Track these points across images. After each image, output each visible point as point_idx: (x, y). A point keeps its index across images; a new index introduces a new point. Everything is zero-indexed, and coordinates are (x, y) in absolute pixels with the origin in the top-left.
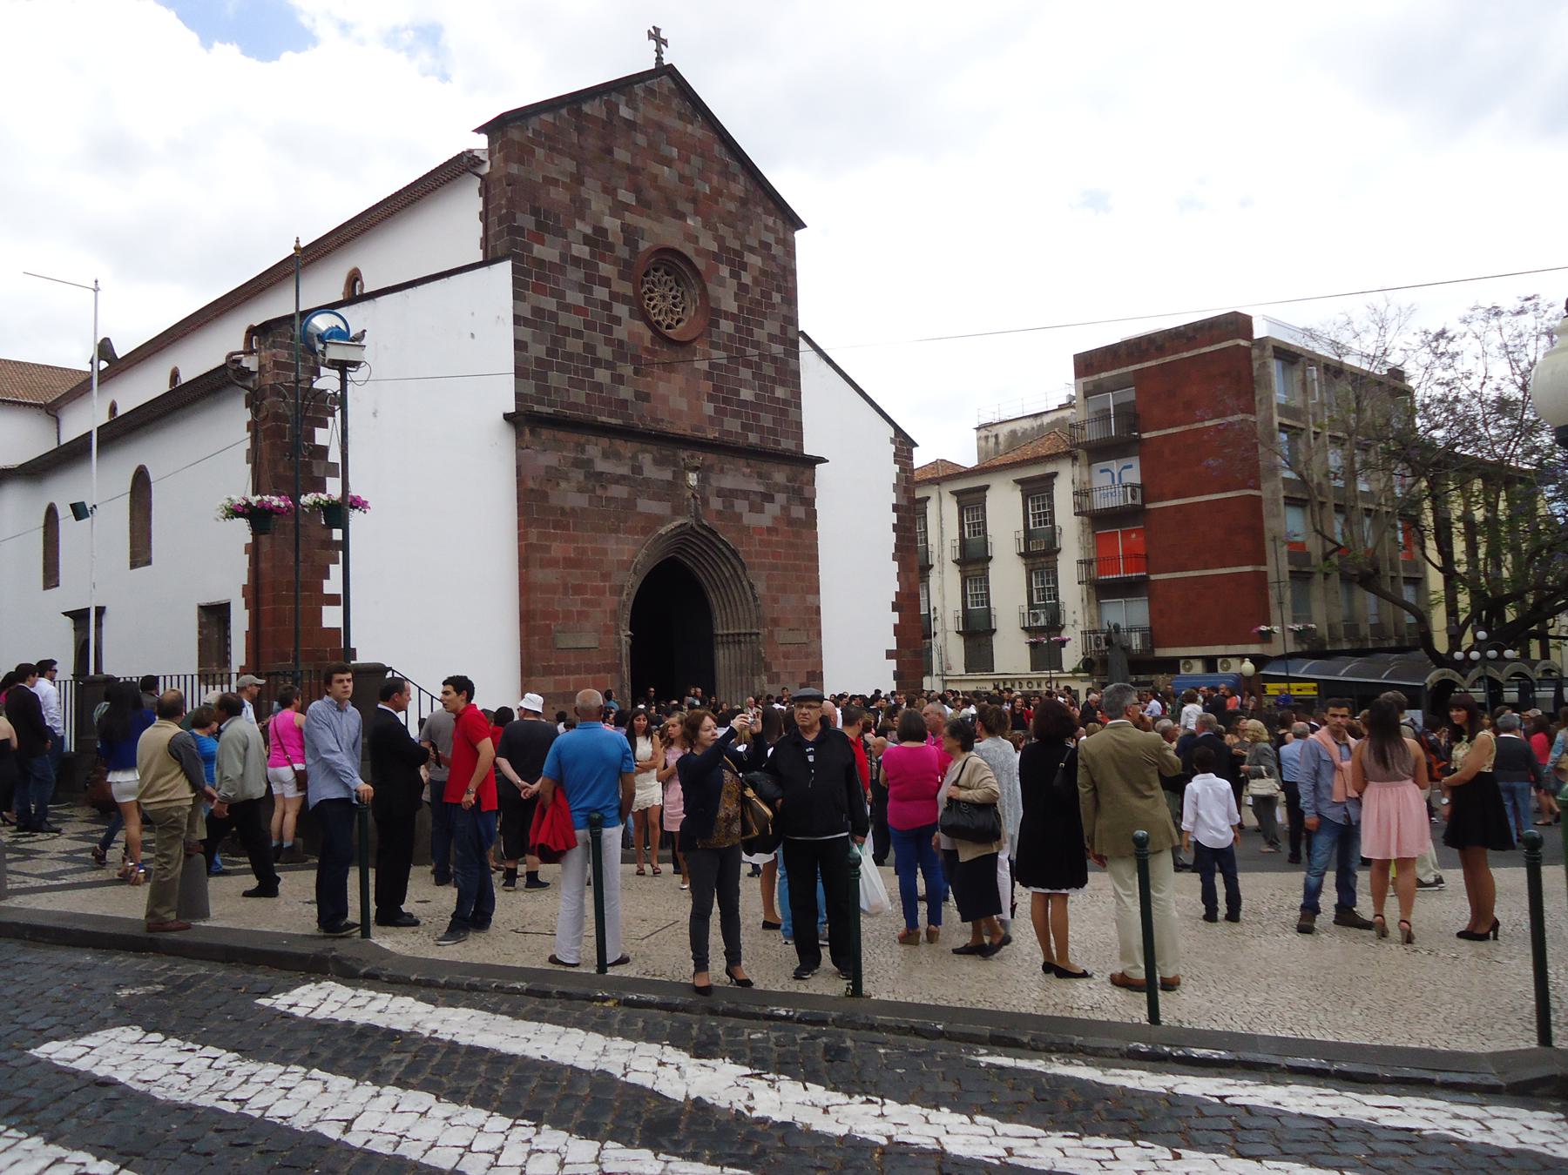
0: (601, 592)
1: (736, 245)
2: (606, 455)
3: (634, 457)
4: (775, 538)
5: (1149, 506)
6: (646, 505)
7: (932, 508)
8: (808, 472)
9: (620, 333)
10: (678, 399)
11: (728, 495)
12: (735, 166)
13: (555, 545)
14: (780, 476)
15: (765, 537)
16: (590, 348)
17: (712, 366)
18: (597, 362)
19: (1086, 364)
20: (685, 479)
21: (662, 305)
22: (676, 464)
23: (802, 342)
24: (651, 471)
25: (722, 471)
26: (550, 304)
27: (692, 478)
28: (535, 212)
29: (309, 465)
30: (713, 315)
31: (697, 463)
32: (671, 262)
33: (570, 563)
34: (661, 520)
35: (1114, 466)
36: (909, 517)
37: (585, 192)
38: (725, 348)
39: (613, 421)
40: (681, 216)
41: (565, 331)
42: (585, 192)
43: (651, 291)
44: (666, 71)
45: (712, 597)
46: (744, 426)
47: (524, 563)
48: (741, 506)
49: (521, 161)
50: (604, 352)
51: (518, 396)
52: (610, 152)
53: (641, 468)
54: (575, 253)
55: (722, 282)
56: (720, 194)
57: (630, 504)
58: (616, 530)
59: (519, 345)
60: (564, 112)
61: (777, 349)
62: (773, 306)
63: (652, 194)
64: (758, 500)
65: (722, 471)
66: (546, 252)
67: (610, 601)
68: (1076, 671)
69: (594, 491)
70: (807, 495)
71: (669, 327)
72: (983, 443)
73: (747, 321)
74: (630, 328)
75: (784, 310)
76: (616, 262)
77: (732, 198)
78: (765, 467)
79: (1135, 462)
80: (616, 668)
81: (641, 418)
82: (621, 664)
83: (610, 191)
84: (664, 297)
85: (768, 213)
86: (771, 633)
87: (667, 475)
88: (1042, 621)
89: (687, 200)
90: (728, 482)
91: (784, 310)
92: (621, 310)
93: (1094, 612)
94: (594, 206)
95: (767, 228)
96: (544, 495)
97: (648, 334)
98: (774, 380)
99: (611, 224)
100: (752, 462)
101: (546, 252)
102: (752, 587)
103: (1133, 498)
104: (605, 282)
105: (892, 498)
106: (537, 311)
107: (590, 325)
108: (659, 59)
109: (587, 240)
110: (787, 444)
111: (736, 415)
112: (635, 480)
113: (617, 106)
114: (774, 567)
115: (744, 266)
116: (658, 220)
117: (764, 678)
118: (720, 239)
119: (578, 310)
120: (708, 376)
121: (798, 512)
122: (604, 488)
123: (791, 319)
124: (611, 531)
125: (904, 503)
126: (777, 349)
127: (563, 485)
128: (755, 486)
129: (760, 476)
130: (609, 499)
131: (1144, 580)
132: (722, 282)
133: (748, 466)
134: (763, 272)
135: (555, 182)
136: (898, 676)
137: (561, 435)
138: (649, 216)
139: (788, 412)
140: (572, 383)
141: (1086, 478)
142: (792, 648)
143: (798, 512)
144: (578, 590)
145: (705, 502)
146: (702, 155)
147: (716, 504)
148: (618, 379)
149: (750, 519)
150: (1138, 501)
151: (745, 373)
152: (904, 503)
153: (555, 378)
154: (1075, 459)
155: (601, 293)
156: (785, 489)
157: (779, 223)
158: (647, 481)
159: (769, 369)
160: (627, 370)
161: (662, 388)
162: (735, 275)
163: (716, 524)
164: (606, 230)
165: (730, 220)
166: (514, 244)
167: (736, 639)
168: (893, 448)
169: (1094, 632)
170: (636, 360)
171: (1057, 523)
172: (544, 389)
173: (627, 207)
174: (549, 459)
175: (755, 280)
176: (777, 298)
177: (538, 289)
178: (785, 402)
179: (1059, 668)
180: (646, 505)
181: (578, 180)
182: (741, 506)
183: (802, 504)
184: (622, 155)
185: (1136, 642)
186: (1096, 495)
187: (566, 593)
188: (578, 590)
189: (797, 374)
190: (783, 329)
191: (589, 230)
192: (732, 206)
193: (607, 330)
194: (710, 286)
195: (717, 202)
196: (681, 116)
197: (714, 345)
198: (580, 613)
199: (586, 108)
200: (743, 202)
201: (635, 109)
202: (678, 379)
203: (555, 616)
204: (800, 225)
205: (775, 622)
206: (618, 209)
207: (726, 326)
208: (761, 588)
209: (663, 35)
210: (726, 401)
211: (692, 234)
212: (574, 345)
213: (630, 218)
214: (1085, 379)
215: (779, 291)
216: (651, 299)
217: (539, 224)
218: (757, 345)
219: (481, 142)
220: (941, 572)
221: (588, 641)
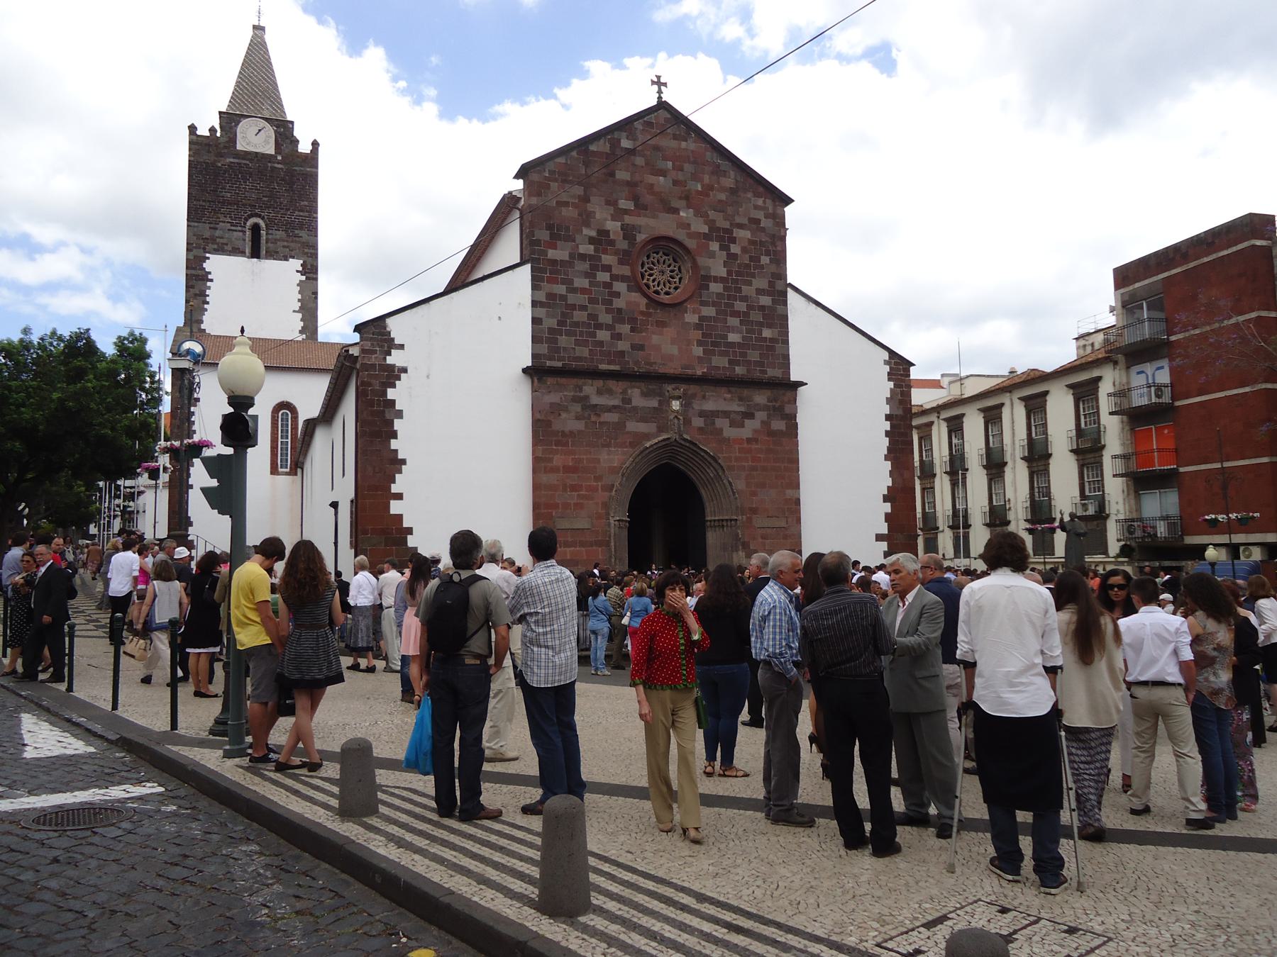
0: (595, 489)
1: (727, 225)
2: (599, 392)
3: (624, 392)
4: (754, 446)
5: (1178, 403)
6: (633, 426)
7: (1006, 413)
8: (789, 394)
9: (619, 303)
10: (669, 346)
11: (709, 416)
12: (725, 165)
13: (556, 457)
14: (760, 398)
15: (745, 445)
16: (593, 317)
17: (701, 318)
18: (599, 326)
19: (1124, 276)
20: (669, 405)
21: (662, 278)
22: (661, 394)
23: (790, 292)
24: (638, 399)
25: (704, 397)
26: (561, 289)
27: (676, 405)
28: (550, 227)
29: (383, 412)
30: (704, 280)
31: (677, 393)
32: (665, 246)
33: (567, 469)
34: (647, 437)
35: (1149, 368)
36: (904, 424)
37: (590, 207)
39: (612, 367)
40: (676, 211)
41: (573, 307)
42: (590, 207)
43: (651, 269)
44: (662, 105)
45: (703, 492)
46: (730, 362)
47: (535, 471)
48: (721, 423)
49: (539, 194)
50: (605, 318)
51: (534, 356)
52: (612, 175)
53: (629, 401)
54: (581, 251)
55: (712, 255)
56: (711, 188)
57: (620, 426)
58: (608, 445)
59: (536, 321)
60: (574, 153)
61: (766, 301)
62: (762, 267)
63: (648, 199)
64: (739, 418)
65: (704, 397)
66: (559, 254)
67: (602, 496)
68: (1118, 556)
69: (589, 418)
70: (788, 410)
71: (667, 293)
72: (1082, 352)
74: (627, 298)
75: (773, 268)
76: (616, 253)
77: (723, 189)
78: (746, 392)
79: (1165, 363)
80: (608, 544)
81: (637, 363)
82: (609, 542)
83: (611, 203)
84: (663, 272)
85: (757, 195)
86: (750, 520)
87: (654, 403)
88: (1091, 511)
89: (680, 198)
90: (710, 406)
91: (773, 268)
92: (620, 287)
93: (1133, 502)
94: (598, 216)
95: (756, 207)
96: (549, 423)
97: (644, 301)
98: (761, 324)
99: (613, 226)
100: (733, 389)
101: (559, 254)
102: (730, 483)
103: (1158, 396)
104: (607, 268)
106: (551, 296)
107: (593, 301)
108: (660, 98)
109: (592, 241)
110: (773, 373)
112: (626, 409)
113: (619, 141)
114: (754, 469)
115: (733, 240)
117: (742, 554)
119: (583, 291)
120: (698, 327)
121: (778, 425)
122: (599, 416)
123: (782, 275)
124: (604, 446)
125: (900, 412)
126: (766, 301)
127: (564, 415)
128: (736, 407)
129: (741, 399)
131: (1174, 473)
132: (712, 255)
133: (730, 392)
134: (751, 242)
135: (566, 204)
137: (563, 381)
138: (645, 216)
139: (778, 349)
140: (577, 343)
141: (1125, 380)
142: (769, 531)
143: (778, 425)
144: (574, 488)
145: (687, 422)
146: (695, 162)
147: (698, 422)
148: (618, 337)
149: (729, 432)
150: (1166, 398)
151: (734, 321)
152: (900, 412)
153: (564, 341)
154: (1116, 363)
155: (603, 277)
156: (766, 408)
157: (769, 202)
158: (635, 409)
159: (756, 316)
160: (625, 329)
161: (655, 339)
162: (722, 248)
163: (697, 438)
164: (606, 233)
165: (720, 207)
166: (533, 252)
167: (721, 524)
168: (887, 368)
169: (1133, 520)
170: (632, 321)
171: (1102, 422)
172: (555, 350)
173: (626, 212)
174: (554, 398)
175: (744, 250)
176: (765, 260)
177: (550, 281)
179: (1105, 553)
180: (633, 426)
181: (585, 199)
182: (721, 423)
183: (783, 419)
184: (622, 175)
185: (1162, 530)
186: (1134, 394)
187: (565, 490)
188: (574, 488)
189: (785, 318)
190: (771, 284)
191: (593, 234)
192: (723, 196)
193: (611, 302)
194: (702, 261)
195: (708, 195)
196: (675, 137)
198: (576, 504)
199: (593, 148)
200: (733, 191)
201: (634, 140)
202: (670, 332)
203: (556, 506)
204: (788, 201)
205: (754, 511)
206: (619, 214)
207: (715, 288)
208: (740, 485)
209: (662, 80)
210: (714, 344)
211: (686, 223)
212: (580, 316)
214: (1122, 291)
215: (768, 253)
216: (651, 275)
217: (552, 235)
218: (744, 299)
219: (519, 184)
220: (1014, 468)
221: (583, 523)
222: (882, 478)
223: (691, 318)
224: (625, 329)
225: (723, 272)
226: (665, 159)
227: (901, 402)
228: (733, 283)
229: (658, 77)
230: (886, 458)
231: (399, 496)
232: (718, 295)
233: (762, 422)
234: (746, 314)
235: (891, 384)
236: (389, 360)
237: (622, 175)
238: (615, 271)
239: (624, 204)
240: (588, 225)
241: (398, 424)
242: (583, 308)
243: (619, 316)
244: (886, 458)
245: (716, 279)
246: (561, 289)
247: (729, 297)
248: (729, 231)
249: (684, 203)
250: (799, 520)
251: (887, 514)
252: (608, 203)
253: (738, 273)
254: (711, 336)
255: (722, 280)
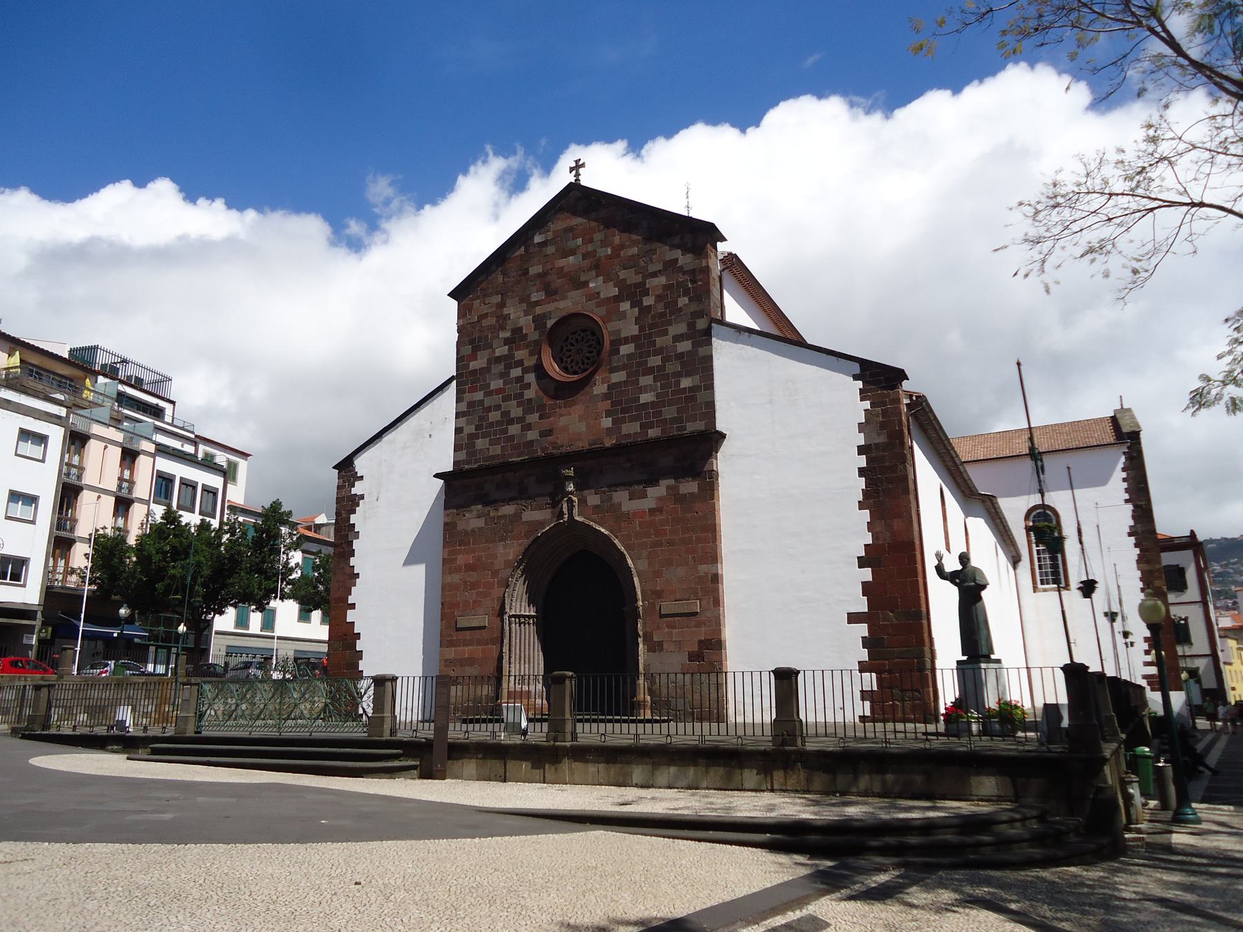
1: (639, 278)
9: (530, 394)
15: (648, 518)
16: (506, 414)
18: (511, 422)
20: (563, 487)
26: (479, 395)
33: (470, 568)
38: (624, 368)
40: (586, 284)
41: (489, 409)
50: (516, 412)
52: (526, 272)
55: (623, 316)
56: (622, 247)
57: (517, 516)
59: (458, 431)
61: (684, 346)
63: (559, 282)
73: (650, 335)
81: (543, 449)
83: (524, 299)
89: (590, 269)
91: (694, 307)
99: (526, 322)
104: (520, 363)
105: (861, 440)
106: (471, 404)
107: (505, 399)
109: (507, 342)
111: (633, 419)
116: (564, 298)
118: (621, 284)
119: (498, 391)
120: (606, 397)
124: (500, 540)
130: (500, 517)
132: (623, 316)
134: (666, 287)
136: (866, 643)
143: (690, 487)
144: (474, 586)
148: (528, 427)
151: (646, 380)
152: (882, 439)
153: (480, 443)
155: (516, 372)
160: (533, 418)
161: (563, 421)
165: (631, 263)
170: (541, 408)
173: (537, 303)
175: (659, 298)
176: (683, 301)
178: (692, 389)
181: (502, 305)
188: (474, 586)
190: (691, 325)
191: (507, 334)
193: (522, 394)
197: (613, 370)
202: (577, 410)
210: (624, 411)
213: (539, 310)
222: (856, 532)
223: (599, 388)
224: (533, 418)
225: (634, 330)
226: (575, 238)
227: (883, 426)
228: (644, 342)
229: (577, 162)
230: (862, 506)
231: (353, 606)
232: (629, 356)
233: (668, 487)
234: (661, 368)
235: (867, 404)
236: (354, 491)
237: (535, 270)
238: (526, 364)
239: (535, 297)
240: (503, 328)
241: (356, 544)
242: (498, 407)
243: (529, 406)
244: (862, 506)
245: (626, 341)
246: (479, 395)
247: (641, 355)
248: (641, 285)
249: (594, 273)
250: (717, 602)
251: (864, 584)
252: (522, 301)
253: (652, 326)
254: (621, 403)
255: (634, 339)
